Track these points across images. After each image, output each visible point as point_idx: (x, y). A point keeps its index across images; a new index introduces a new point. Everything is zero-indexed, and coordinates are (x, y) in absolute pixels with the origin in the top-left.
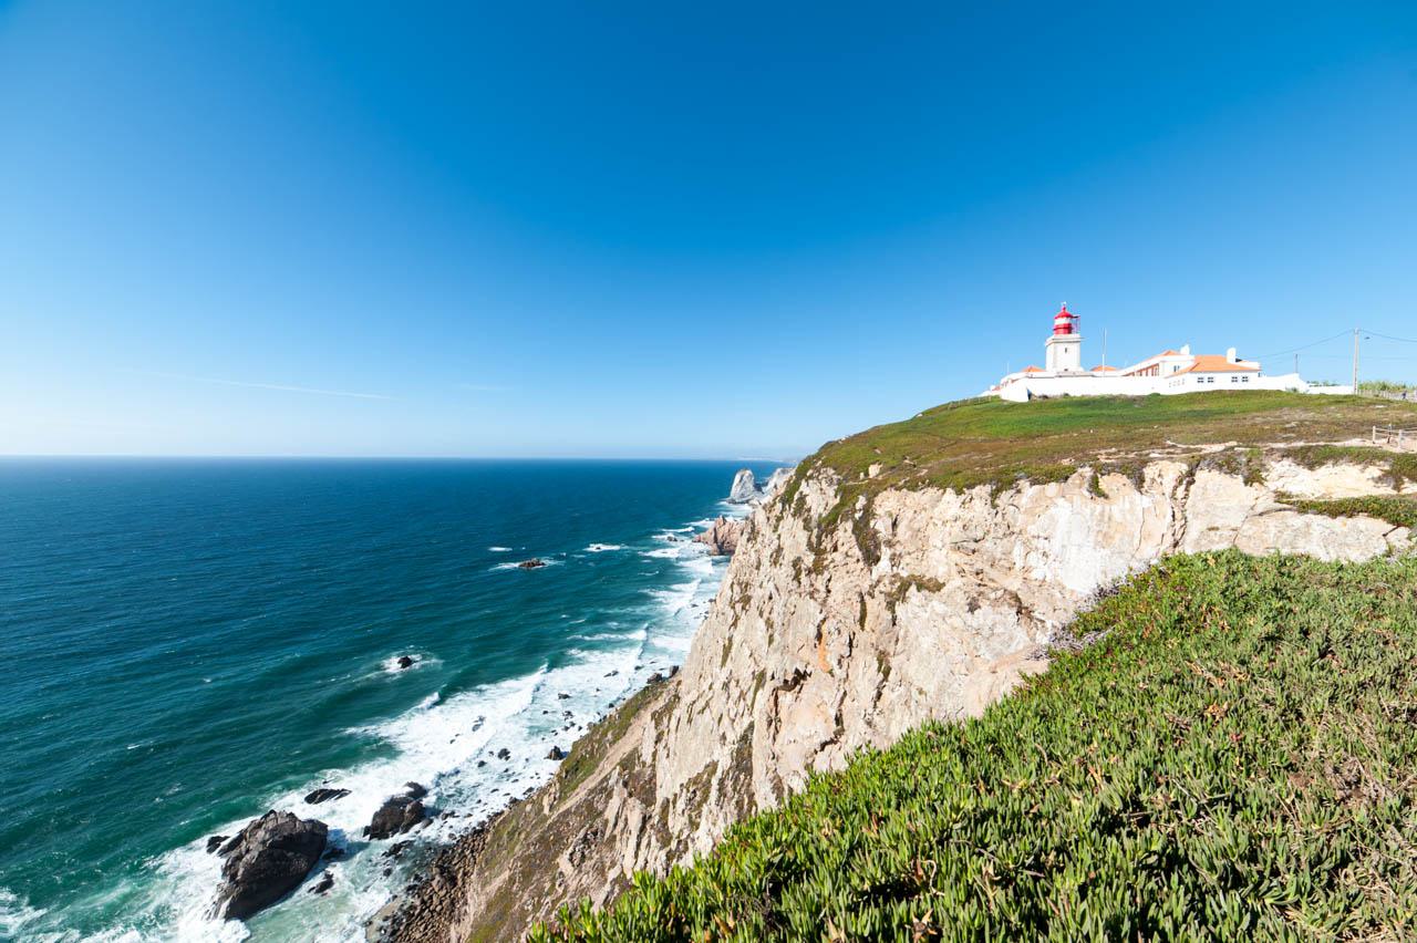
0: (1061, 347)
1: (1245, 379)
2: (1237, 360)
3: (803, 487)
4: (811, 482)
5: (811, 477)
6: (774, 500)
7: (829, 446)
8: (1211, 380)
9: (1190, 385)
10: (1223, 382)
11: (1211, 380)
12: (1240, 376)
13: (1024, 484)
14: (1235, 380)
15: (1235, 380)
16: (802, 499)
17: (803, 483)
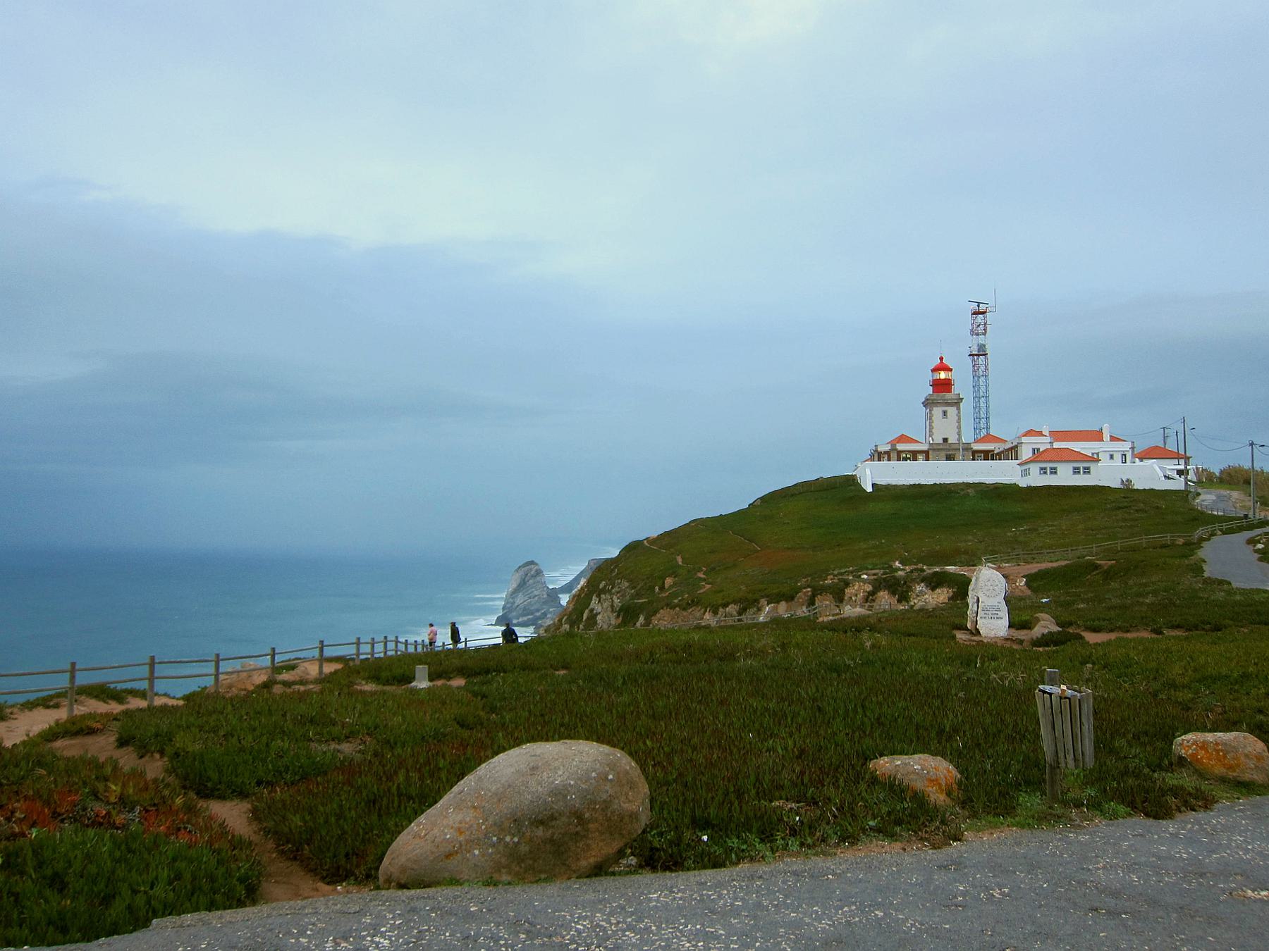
0: (937, 411)
1: (1087, 471)
2: (1113, 439)
3: (594, 603)
4: (603, 596)
5: (604, 591)
6: (560, 620)
7: (633, 549)
8: (1054, 471)
9: (1036, 479)
10: (1065, 476)
11: (1054, 471)
12: (1081, 465)
13: (763, 601)
14: (1076, 471)
15: (1076, 471)
16: (593, 617)
17: (595, 599)
